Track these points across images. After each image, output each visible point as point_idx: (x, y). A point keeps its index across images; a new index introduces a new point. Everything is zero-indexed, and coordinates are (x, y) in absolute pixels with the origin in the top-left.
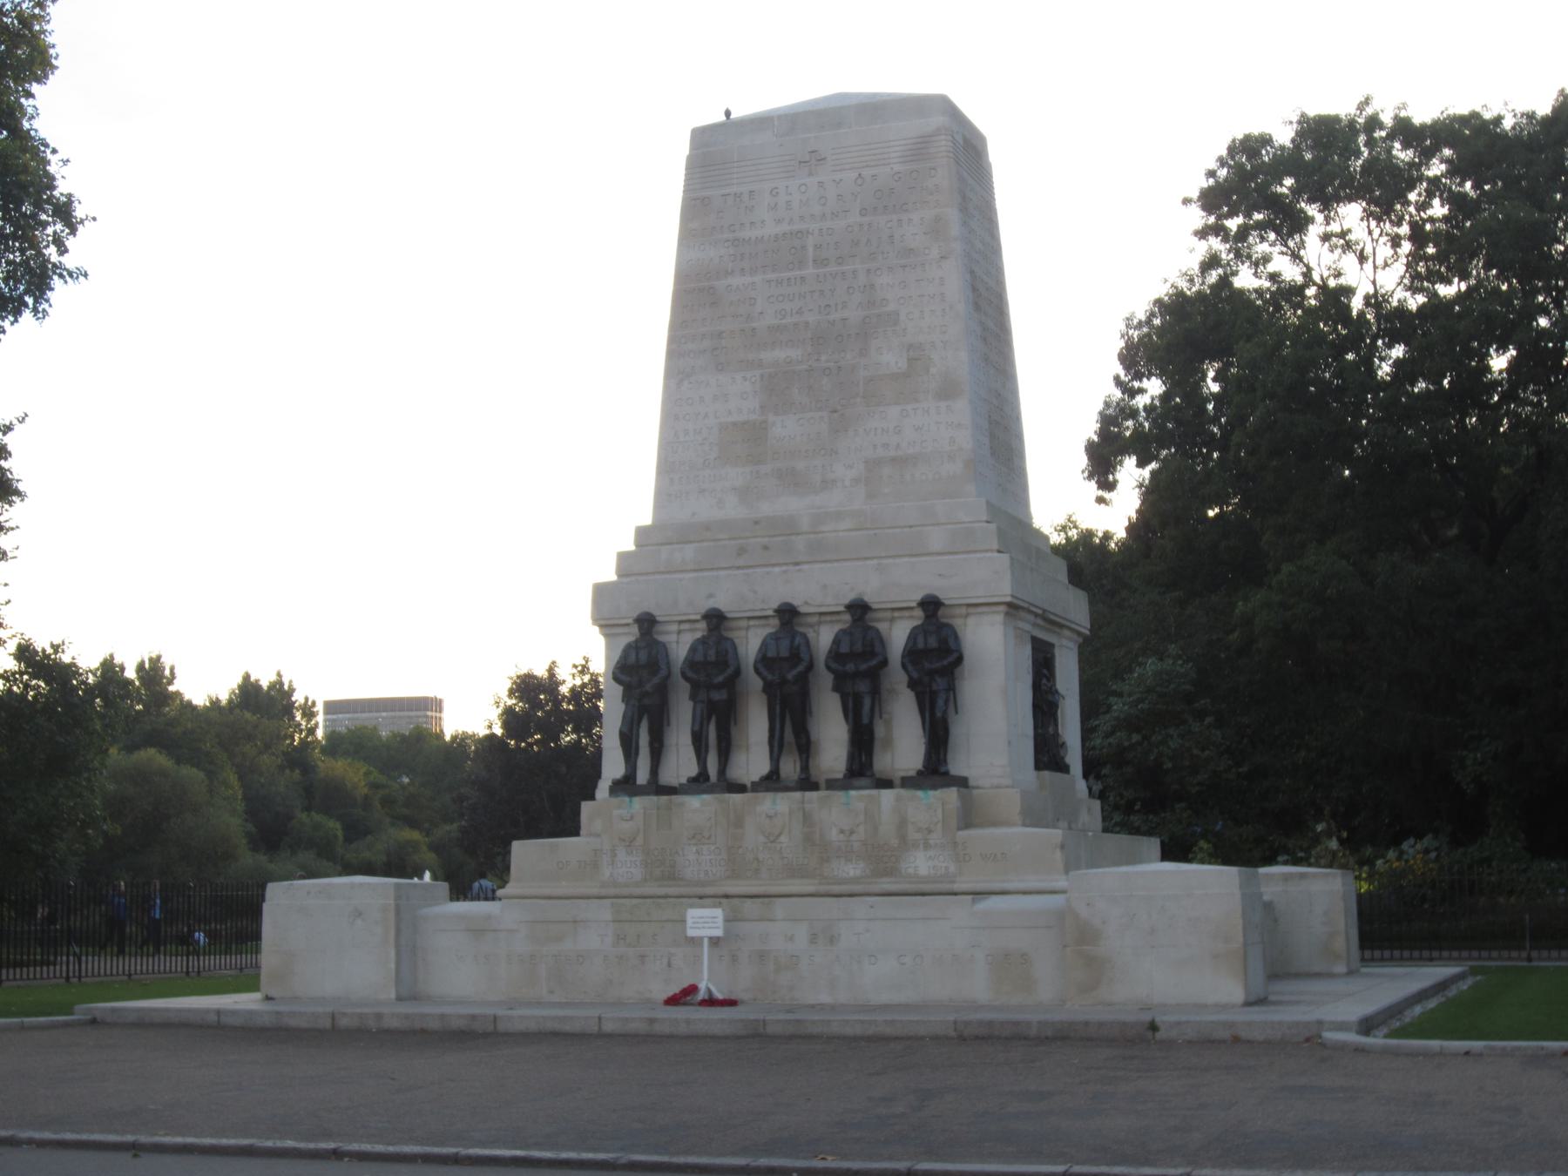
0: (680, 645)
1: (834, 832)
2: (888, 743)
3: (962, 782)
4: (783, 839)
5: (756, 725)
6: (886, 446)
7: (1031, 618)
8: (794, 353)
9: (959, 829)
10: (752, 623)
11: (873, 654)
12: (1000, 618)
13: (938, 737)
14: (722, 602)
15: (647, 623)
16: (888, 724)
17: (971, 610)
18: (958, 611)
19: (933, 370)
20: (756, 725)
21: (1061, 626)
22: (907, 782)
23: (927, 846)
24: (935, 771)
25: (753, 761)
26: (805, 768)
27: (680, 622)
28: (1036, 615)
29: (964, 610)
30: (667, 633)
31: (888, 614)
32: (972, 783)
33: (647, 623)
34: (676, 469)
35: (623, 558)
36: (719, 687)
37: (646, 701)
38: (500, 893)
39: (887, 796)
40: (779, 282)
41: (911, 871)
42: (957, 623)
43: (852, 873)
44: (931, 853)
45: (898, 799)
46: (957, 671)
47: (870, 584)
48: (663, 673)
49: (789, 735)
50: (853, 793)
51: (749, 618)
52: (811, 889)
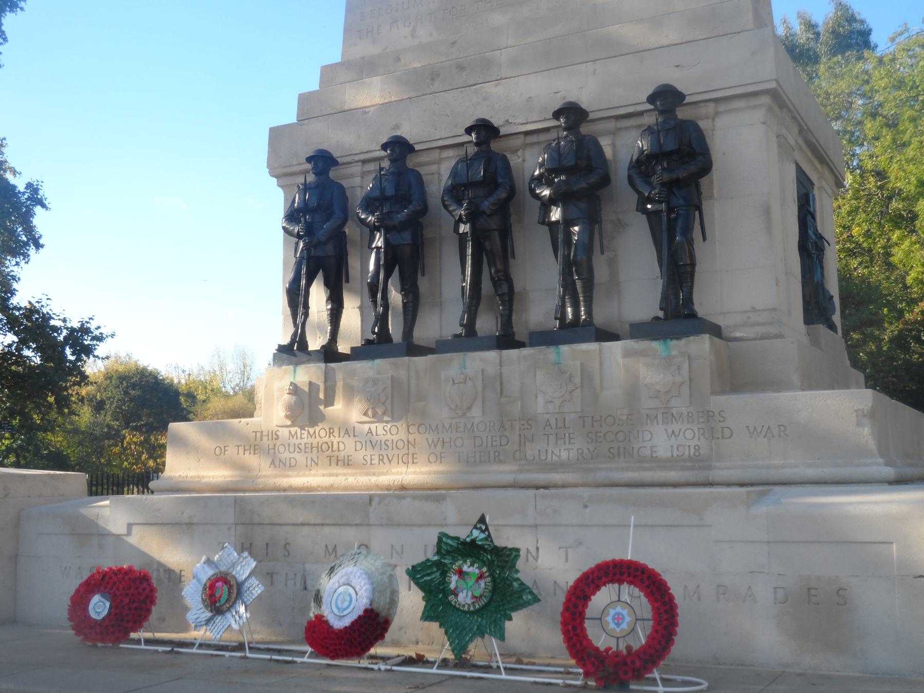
0: (359, 183)
2: (614, 284)
5: (451, 276)
9: (714, 393)
10: (445, 154)
11: (589, 169)
12: (758, 115)
13: (679, 272)
14: (408, 132)
15: (323, 161)
16: (612, 264)
17: (722, 107)
18: (702, 110)
20: (451, 276)
22: (640, 331)
23: (669, 416)
24: (679, 314)
25: (441, 320)
26: (507, 323)
27: (364, 162)
30: (352, 176)
31: (611, 125)
33: (323, 161)
39: (615, 348)
41: (647, 452)
43: (564, 455)
44: (675, 427)
46: (704, 181)
47: (586, 88)
49: (487, 286)
50: (564, 348)
51: (442, 148)
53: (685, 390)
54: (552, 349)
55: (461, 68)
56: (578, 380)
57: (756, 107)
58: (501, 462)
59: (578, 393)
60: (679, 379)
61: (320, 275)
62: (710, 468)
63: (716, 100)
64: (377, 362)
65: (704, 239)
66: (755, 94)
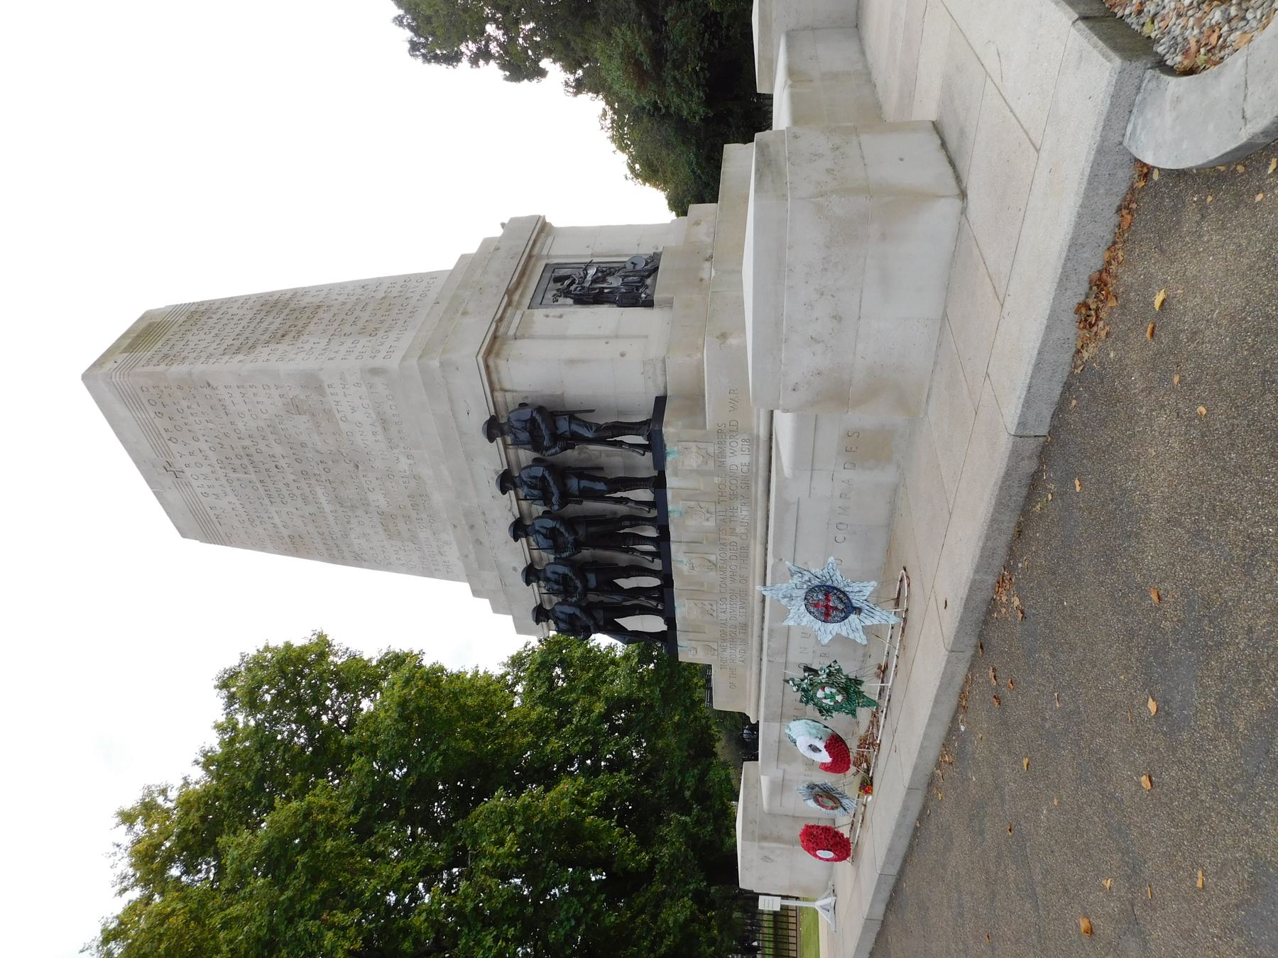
1: (707, 524)
3: (661, 402)
4: (713, 558)
6: (374, 434)
7: (510, 311)
8: (319, 491)
9: (704, 427)
17: (497, 386)
19: (302, 397)
21: (530, 256)
23: (722, 454)
28: (509, 304)
29: (498, 395)
32: (660, 393)
34: (430, 567)
35: (496, 609)
36: (585, 581)
37: (602, 623)
38: (753, 721)
39: (671, 481)
40: (270, 496)
41: (745, 469)
42: (512, 400)
44: (728, 452)
45: (676, 474)
48: (578, 612)
50: (670, 508)
52: (759, 549)
53: (702, 445)
54: (671, 515)
55: (472, 527)
56: (692, 504)
58: (748, 546)
59: (702, 504)
60: (694, 449)
61: (618, 620)
62: (758, 436)
63: (492, 391)
64: (676, 604)
66: (487, 367)
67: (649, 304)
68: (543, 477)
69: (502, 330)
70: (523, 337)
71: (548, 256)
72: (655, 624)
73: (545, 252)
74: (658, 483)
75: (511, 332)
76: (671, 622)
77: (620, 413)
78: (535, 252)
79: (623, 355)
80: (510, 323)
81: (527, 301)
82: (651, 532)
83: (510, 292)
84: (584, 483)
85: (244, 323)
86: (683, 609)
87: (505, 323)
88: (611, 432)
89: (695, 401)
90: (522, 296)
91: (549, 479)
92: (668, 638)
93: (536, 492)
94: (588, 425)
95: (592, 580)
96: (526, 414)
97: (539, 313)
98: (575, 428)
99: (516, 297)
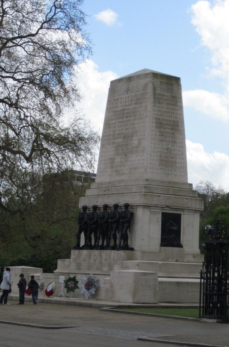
3: (132, 249)
7: (160, 208)
17: (137, 207)
32: (135, 249)
39: (113, 251)
50: (107, 251)
57: (141, 207)
63: (136, 206)
65: (130, 232)
67: (162, 245)
68: (115, 217)
69: (153, 208)
70: (151, 213)
71: (184, 214)
72: (82, 243)
73: (185, 213)
74: (114, 248)
75: (152, 210)
76: (83, 248)
77: (131, 238)
78: (185, 210)
79: (143, 240)
80: (156, 209)
81: (165, 211)
82: (105, 244)
83: (167, 207)
84: (114, 229)
85: (170, 119)
86: (85, 252)
87: (155, 208)
88: (125, 238)
89: (130, 258)
90: (166, 210)
91: (115, 219)
92: (78, 247)
93: (112, 216)
94: (126, 231)
95: (93, 226)
96: (129, 216)
97: (160, 216)
98: (125, 228)
99: (166, 208)
